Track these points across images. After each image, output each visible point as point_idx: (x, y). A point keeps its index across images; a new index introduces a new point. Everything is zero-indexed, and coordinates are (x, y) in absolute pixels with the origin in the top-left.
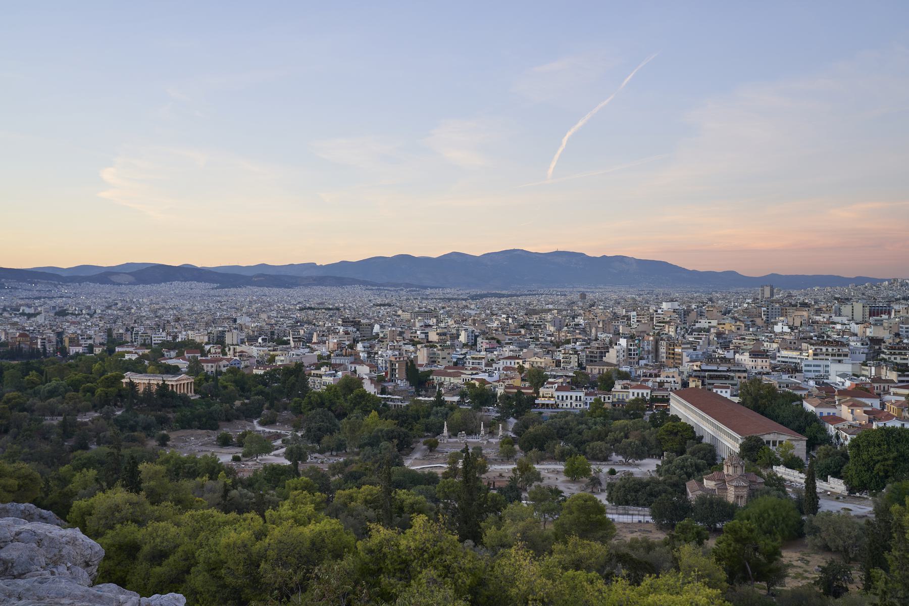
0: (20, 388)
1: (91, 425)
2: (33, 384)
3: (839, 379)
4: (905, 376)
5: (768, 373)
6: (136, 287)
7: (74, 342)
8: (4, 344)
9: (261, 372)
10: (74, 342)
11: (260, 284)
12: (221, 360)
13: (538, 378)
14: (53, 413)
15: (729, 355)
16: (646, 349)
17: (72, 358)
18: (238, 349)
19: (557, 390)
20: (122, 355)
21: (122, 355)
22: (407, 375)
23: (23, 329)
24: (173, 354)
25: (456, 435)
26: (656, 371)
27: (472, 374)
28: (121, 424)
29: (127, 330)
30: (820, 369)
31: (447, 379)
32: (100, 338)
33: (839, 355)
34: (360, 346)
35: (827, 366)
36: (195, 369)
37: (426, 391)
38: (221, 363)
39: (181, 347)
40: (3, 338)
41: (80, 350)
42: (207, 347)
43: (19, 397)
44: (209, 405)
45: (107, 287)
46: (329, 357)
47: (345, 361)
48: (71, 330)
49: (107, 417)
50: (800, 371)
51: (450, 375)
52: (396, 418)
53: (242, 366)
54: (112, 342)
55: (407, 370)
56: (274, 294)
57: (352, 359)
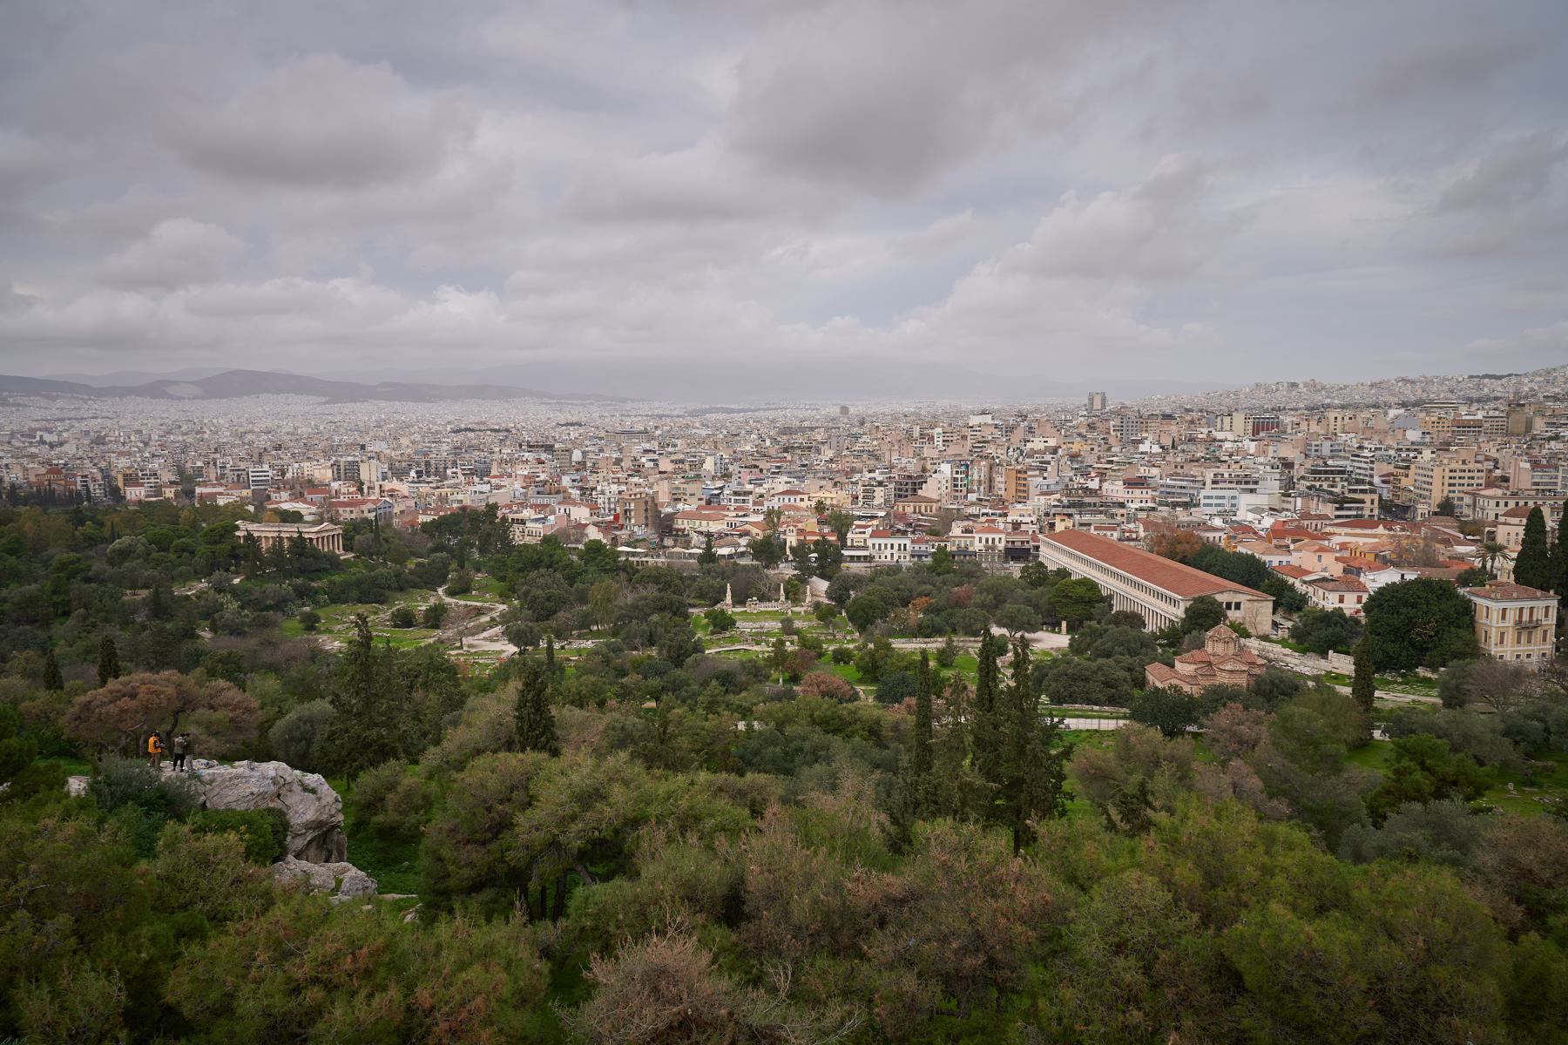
3: (1250, 516)
4: (1341, 508)
7: (131, 480)
9: (428, 519)
12: (364, 502)
13: (841, 523)
15: (1094, 485)
16: (976, 477)
18: (387, 485)
19: (871, 536)
20: (213, 496)
24: (285, 495)
31: (704, 523)
32: (167, 476)
34: (566, 481)
35: (1234, 498)
36: (328, 512)
38: (364, 507)
47: (552, 500)
48: (123, 463)
51: (708, 518)
54: (187, 481)
57: (560, 497)
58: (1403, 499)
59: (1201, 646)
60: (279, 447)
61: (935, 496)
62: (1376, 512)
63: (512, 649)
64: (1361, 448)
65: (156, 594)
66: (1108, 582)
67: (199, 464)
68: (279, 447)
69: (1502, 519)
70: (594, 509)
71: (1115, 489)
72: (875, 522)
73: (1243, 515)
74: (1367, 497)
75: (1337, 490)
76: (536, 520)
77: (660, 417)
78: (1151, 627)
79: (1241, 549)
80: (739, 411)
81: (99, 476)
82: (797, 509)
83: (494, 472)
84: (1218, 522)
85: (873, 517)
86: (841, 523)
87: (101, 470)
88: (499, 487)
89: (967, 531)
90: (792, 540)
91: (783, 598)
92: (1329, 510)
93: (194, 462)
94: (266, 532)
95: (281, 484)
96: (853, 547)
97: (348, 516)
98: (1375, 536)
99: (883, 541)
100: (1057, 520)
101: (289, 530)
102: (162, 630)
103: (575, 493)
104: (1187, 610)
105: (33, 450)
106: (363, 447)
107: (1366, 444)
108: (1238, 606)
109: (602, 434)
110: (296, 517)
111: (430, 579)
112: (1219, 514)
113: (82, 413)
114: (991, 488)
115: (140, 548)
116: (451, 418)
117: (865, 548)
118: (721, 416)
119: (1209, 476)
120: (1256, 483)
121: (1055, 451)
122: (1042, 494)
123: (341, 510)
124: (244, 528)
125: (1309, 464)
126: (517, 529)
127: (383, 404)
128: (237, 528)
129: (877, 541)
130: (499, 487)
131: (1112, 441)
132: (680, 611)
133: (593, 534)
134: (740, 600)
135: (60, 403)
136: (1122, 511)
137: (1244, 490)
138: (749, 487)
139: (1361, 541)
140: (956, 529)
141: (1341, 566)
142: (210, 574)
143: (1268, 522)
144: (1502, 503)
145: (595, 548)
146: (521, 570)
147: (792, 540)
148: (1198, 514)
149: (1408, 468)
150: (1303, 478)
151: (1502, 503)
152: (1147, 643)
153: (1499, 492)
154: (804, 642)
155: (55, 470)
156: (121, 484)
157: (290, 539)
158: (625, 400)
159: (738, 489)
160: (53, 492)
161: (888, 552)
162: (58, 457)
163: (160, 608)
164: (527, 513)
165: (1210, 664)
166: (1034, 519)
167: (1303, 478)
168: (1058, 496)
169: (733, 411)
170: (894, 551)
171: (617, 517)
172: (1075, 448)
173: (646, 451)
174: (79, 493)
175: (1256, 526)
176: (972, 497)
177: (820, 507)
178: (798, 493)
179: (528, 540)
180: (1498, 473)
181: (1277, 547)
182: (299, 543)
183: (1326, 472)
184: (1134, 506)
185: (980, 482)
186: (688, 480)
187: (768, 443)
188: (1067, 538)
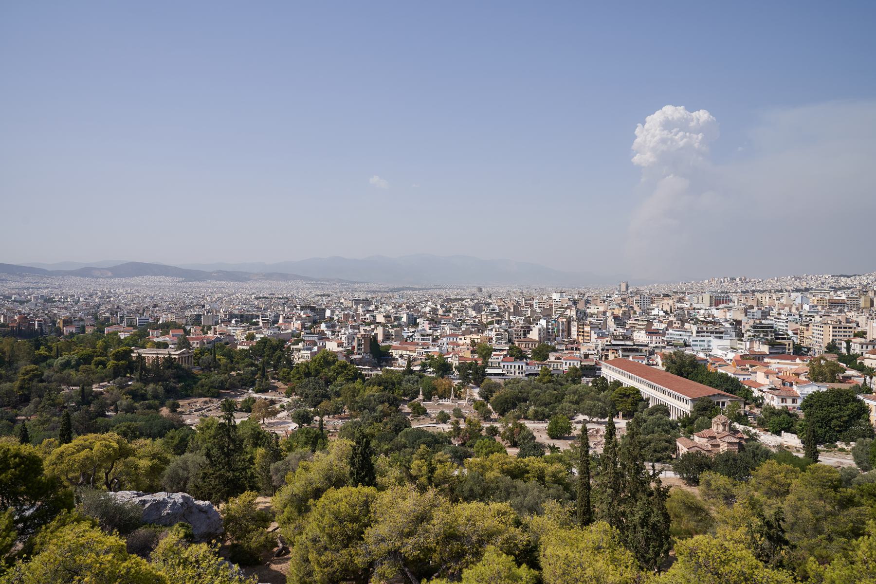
0: (35, 362)
1: (106, 395)
2: (45, 358)
5: (664, 347)
8: (3, 325)
10: (67, 323)
11: (218, 279)
14: (69, 384)
17: (66, 337)
21: (116, 334)
23: (20, 313)
25: (430, 400)
26: (575, 346)
28: (136, 395)
29: (111, 314)
30: (705, 343)
31: (404, 352)
32: (89, 320)
33: (717, 333)
36: (184, 343)
37: (387, 362)
39: (166, 328)
40: (2, 321)
41: (74, 330)
42: (188, 328)
43: (36, 369)
44: (208, 377)
45: (87, 280)
46: (300, 335)
48: (64, 314)
49: (121, 387)
50: (689, 346)
51: (406, 349)
52: (379, 385)
53: (223, 343)
56: (230, 286)
58: (806, 343)
59: (709, 427)
60: (155, 306)
61: (537, 338)
62: (791, 351)
63: (294, 426)
64: (779, 314)
65: (83, 390)
66: (646, 391)
67: (107, 314)
68: (155, 306)
69: (867, 356)
70: (340, 345)
71: (640, 337)
72: (505, 353)
73: (716, 352)
74: (786, 342)
75: (769, 338)
76: (307, 349)
78: (673, 417)
79: (720, 370)
81: (48, 321)
82: (458, 345)
83: (281, 321)
84: (701, 355)
85: (503, 350)
86: (486, 352)
87: (50, 317)
89: (558, 358)
90: (455, 362)
91: (453, 397)
92: (765, 349)
93: (104, 312)
95: (156, 327)
96: (492, 367)
98: (796, 364)
99: (509, 364)
100: (610, 353)
102: (87, 411)
103: (328, 333)
104: (694, 407)
105: (10, 306)
106: (203, 306)
107: (782, 311)
108: (723, 404)
110: (165, 345)
112: (703, 350)
113: (40, 285)
114: (569, 334)
115: (73, 363)
117: (499, 367)
119: (694, 329)
120: (722, 333)
121: (604, 313)
122: (599, 337)
123: (191, 342)
125: (751, 322)
126: (296, 355)
131: (636, 308)
132: (395, 403)
133: (342, 359)
134: (428, 397)
135: (28, 279)
136: (646, 348)
137: (716, 337)
138: (430, 332)
139: (789, 367)
140: (552, 357)
141: (780, 381)
143: (731, 355)
144: (865, 346)
146: (298, 379)
147: (455, 362)
148: (688, 352)
149: (808, 325)
150: (748, 330)
151: (865, 346)
152: (673, 426)
153: (863, 340)
154: (470, 423)
155: (24, 318)
156: (61, 326)
159: (423, 332)
160: (20, 330)
162: (25, 309)
163: (86, 398)
164: (301, 345)
165: (715, 438)
166: (596, 351)
167: (748, 330)
168: (609, 339)
170: (517, 370)
171: (353, 348)
172: (616, 312)
174: (36, 332)
175: (724, 358)
176: (559, 339)
177: (473, 343)
178: (457, 336)
180: (859, 329)
181: (743, 369)
183: (762, 327)
184: (653, 345)
185: (563, 331)
186: (393, 327)
188: (616, 363)
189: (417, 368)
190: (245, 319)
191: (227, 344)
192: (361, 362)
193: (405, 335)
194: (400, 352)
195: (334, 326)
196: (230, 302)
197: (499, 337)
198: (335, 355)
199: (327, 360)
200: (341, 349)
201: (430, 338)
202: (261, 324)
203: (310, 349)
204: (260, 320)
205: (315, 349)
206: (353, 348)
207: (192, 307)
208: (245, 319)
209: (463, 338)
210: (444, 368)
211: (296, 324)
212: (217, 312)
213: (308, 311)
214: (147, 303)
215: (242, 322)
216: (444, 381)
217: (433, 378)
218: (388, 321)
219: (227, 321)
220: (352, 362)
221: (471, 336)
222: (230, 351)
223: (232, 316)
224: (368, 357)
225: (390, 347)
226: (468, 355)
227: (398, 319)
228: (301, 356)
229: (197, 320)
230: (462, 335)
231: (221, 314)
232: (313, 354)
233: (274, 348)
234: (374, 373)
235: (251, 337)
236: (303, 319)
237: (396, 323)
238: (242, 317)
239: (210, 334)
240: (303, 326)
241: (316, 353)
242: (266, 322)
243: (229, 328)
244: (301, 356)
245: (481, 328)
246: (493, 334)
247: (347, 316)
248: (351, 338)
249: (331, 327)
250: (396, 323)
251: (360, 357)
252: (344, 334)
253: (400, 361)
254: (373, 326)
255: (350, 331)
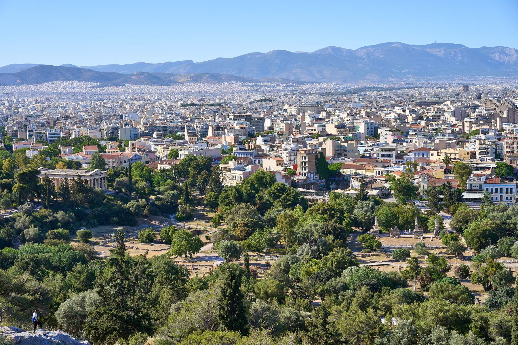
6: (20, 87)
22: (317, 168)
27: (384, 166)
31: (359, 171)
39: (79, 143)
42: (103, 143)
51: (361, 168)
55: (317, 163)
56: (153, 91)
60: (67, 117)
67: (15, 129)
70: (280, 163)
72: (488, 172)
77: (328, 94)
80: (386, 90)
83: (210, 133)
85: (488, 168)
88: (213, 145)
94: (58, 175)
96: (471, 191)
97: (111, 165)
99: (494, 187)
101: (73, 172)
103: (266, 148)
106: (121, 117)
109: (286, 107)
110: (78, 165)
111: (167, 210)
116: (179, 97)
117: (481, 191)
118: (373, 94)
124: (44, 172)
126: (226, 175)
127: (134, 87)
128: (39, 172)
129: (490, 187)
130: (213, 145)
133: (280, 181)
138: (392, 145)
142: (22, 203)
145: (283, 189)
157: (73, 180)
158: (302, 83)
161: (498, 195)
164: (232, 164)
169: (381, 90)
173: (318, 119)
178: (430, 150)
179: (233, 183)
182: (80, 183)
186: (347, 140)
187: (407, 112)
189: (375, 192)
190: (167, 132)
191: (147, 162)
192: (306, 184)
193: (361, 150)
194: (354, 171)
195: (273, 140)
196: (152, 112)
197: (484, 151)
198: (272, 176)
199: (264, 180)
200: (280, 169)
201: (394, 153)
202: (187, 138)
203: (243, 169)
204: (186, 133)
205: (249, 168)
206: (295, 167)
207: (108, 119)
208: (167, 132)
209: (435, 153)
210: (408, 191)
211: (229, 139)
212: (136, 123)
213: (243, 121)
214: (59, 113)
215: (165, 135)
216: (409, 207)
217: (394, 205)
218: (341, 133)
219: (147, 134)
220: (294, 185)
221: (447, 151)
222: (150, 171)
223: (153, 128)
224: (314, 178)
225: (342, 165)
226: (441, 175)
227: (352, 129)
228: (232, 177)
229: (113, 136)
230: (434, 150)
231: (141, 128)
232: (247, 175)
233: (199, 168)
234: (320, 199)
235: (175, 155)
236: (236, 131)
237: (350, 135)
238: (165, 128)
239: (128, 151)
240: (236, 140)
241: (250, 173)
242: (193, 133)
243: (150, 143)
244: (232, 177)
245: (461, 138)
246: (475, 147)
247: (289, 127)
248: (294, 153)
249: (270, 140)
250: (350, 135)
251: (304, 177)
252: (285, 149)
253: (355, 183)
254: (321, 139)
255: (292, 145)
